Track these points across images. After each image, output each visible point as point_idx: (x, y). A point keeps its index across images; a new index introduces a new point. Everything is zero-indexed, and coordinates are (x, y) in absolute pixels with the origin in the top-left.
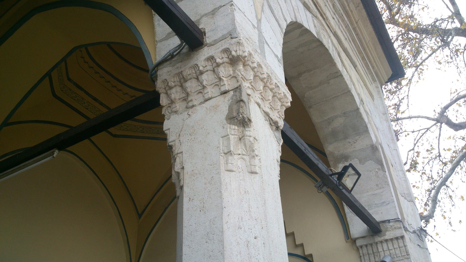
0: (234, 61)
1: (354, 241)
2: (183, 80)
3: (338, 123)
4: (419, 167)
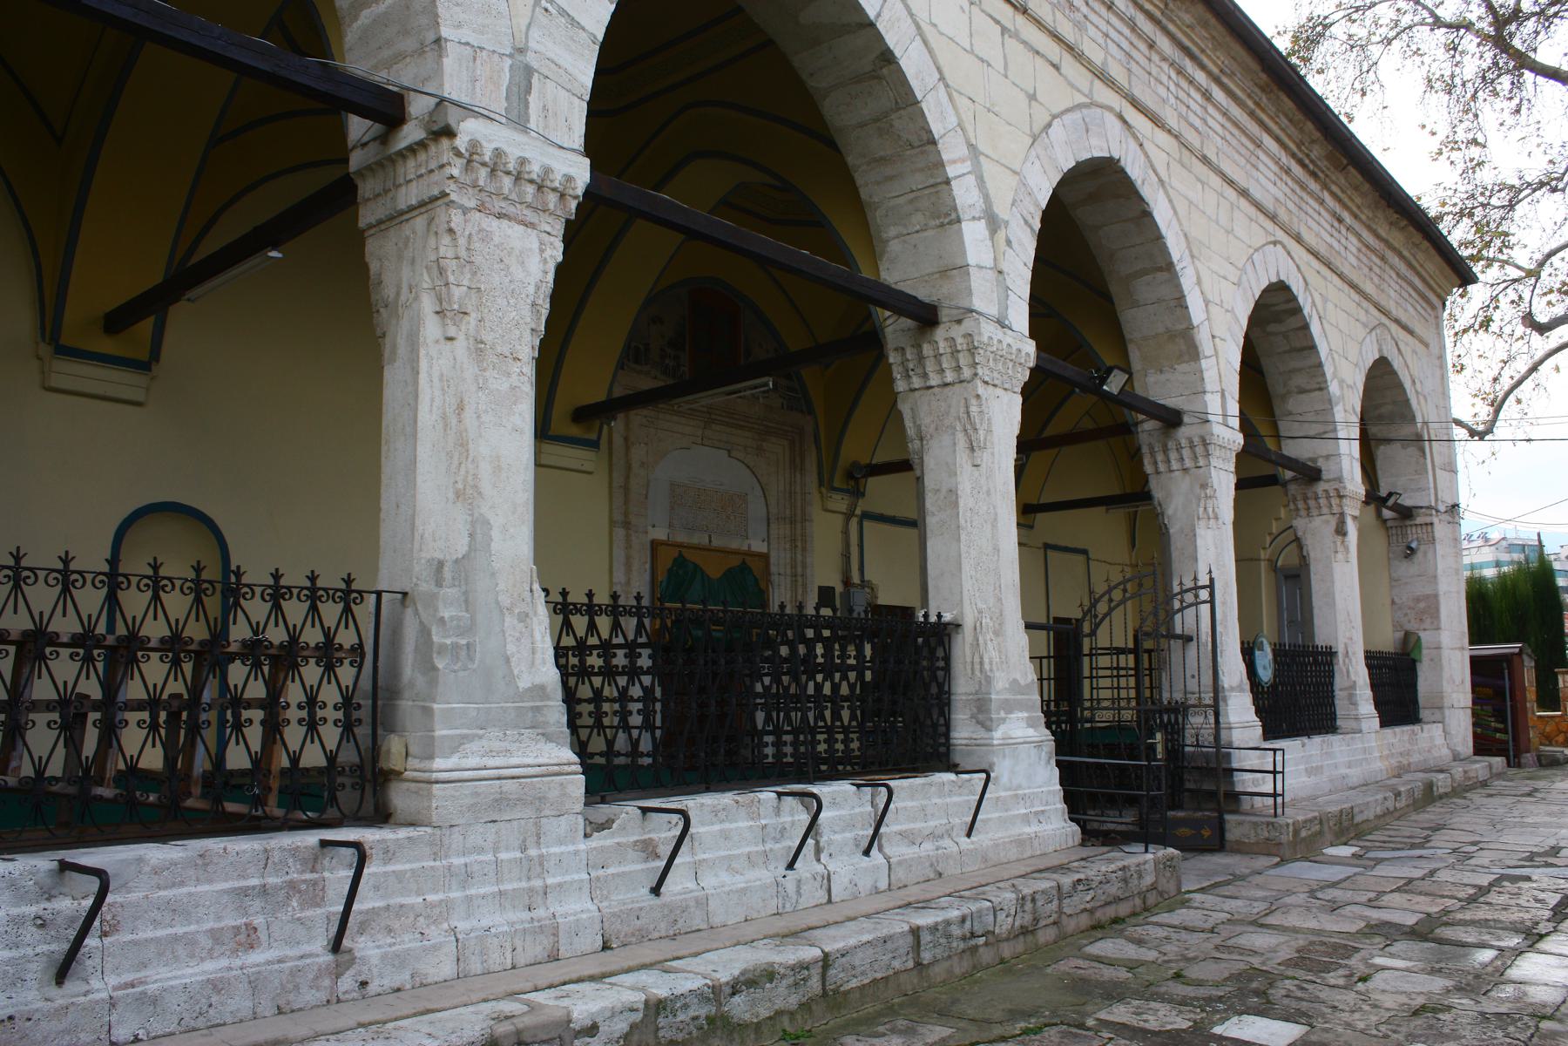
0: (1341, 497)
1: (1385, 521)
2: (1305, 499)
3: (1384, 410)
4: (1494, 327)
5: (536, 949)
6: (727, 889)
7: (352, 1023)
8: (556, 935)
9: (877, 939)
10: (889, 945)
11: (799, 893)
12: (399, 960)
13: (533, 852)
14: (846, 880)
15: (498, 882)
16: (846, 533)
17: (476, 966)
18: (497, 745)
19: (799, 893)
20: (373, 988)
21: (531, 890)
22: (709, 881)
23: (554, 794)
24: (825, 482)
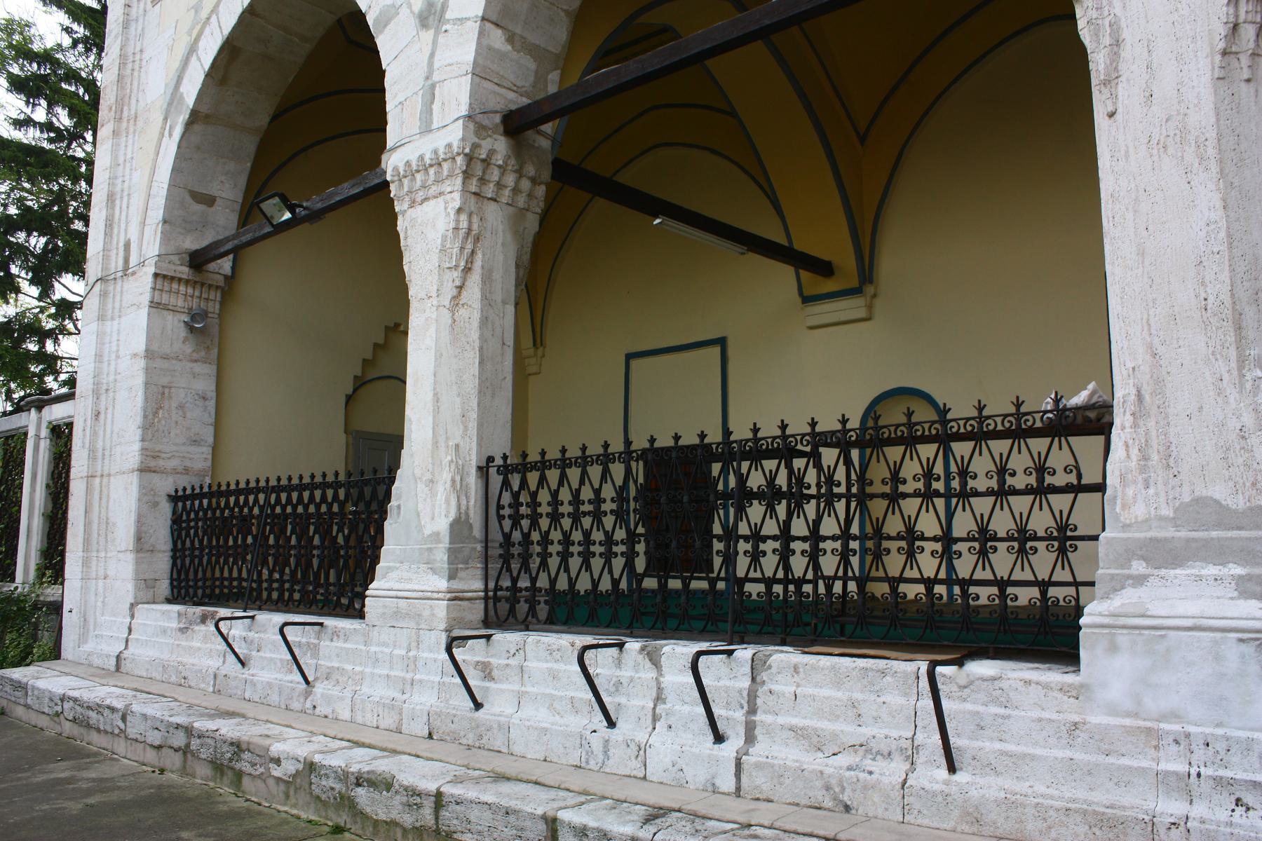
5: (388, 721)
6: (528, 723)
7: (265, 718)
8: (401, 714)
9: (499, 807)
10: (512, 818)
11: (606, 752)
12: (328, 699)
13: (411, 654)
14: (667, 761)
15: (391, 668)
17: (359, 719)
18: (405, 574)
19: (606, 752)
20: (317, 711)
21: (404, 679)
22: (528, 711)
23: (426, 613)
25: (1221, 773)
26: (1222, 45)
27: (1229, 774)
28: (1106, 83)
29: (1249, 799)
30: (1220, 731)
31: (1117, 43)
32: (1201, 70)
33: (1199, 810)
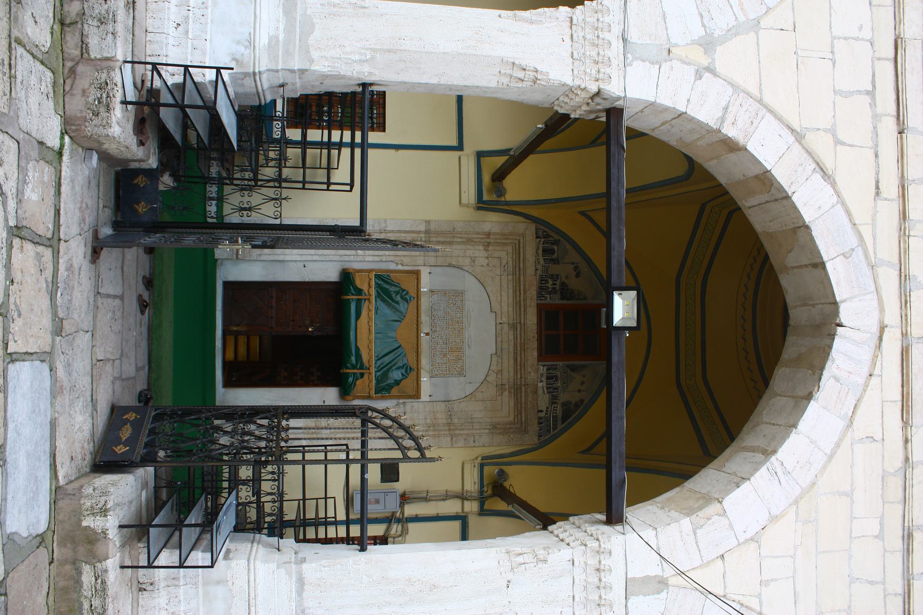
16: (446, 496)
24: (485, 462)
25: (191, 20)
26: (517, 62)
27: (191, 23)
28: (515, 15)
29: (180, 28)
30: (209, 21)
31: (532, 22)
32: (510, 54)
33: (173, 9)
